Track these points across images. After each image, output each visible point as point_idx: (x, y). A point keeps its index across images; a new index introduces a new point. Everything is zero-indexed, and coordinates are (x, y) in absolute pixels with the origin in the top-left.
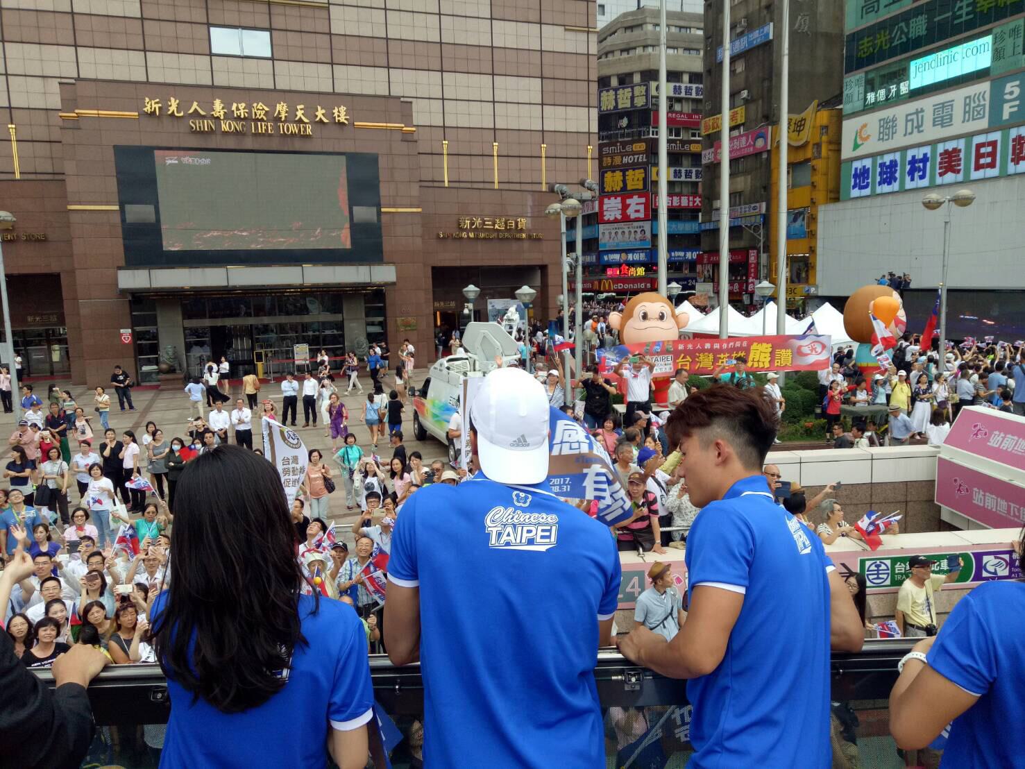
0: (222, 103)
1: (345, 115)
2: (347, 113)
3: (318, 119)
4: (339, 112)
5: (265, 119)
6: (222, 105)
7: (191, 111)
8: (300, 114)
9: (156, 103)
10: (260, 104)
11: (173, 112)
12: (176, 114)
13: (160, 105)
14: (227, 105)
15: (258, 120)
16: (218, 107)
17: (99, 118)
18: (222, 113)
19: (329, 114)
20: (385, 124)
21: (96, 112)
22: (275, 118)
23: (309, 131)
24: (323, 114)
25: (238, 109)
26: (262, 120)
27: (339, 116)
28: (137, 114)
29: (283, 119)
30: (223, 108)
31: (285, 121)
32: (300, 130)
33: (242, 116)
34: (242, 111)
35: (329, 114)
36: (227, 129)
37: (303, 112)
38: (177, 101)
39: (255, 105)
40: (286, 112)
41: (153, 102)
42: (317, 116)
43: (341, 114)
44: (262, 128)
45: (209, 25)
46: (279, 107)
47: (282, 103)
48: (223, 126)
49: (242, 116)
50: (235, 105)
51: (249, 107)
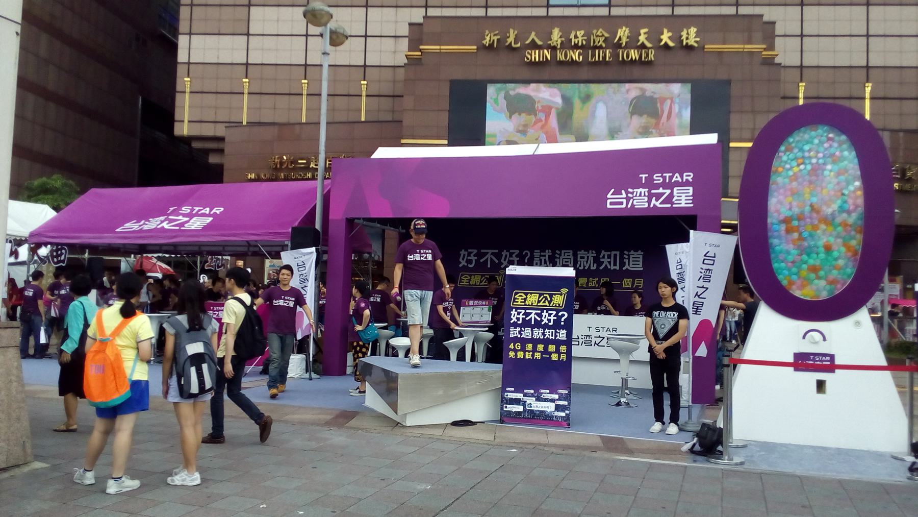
0: (560, 31)
1: (695, 37)
2: (698, 34)
3: (662, 43)
4: (688, 34)
5: (604, 45)
6: (560, 34)
7: (528, 42)
8: (642, 38)
9: (494, 35)
11: (511, 42)
13: (499, 37)
14: (565, 34)
15: (596, 47)
16: (556, 36)
17: (440, 54)
19: (678, 39)
20: (742, 46)
21: (438, 47)
23: (651, 57)
24: (669, 38)
26: (600, 47)
27: (687, 38)
28: (475, 47)
29: (624, 45)
30: (560, 37)
32: (641, 57)
33: (580, 44)
36: (563, 58)
38: (516, 32)
39: (595, 31)
40: (628, 37)
42: (661, 40)
43: (691, 36)
44: (598, 55)
47: (624, 28)
49: (580, 44)
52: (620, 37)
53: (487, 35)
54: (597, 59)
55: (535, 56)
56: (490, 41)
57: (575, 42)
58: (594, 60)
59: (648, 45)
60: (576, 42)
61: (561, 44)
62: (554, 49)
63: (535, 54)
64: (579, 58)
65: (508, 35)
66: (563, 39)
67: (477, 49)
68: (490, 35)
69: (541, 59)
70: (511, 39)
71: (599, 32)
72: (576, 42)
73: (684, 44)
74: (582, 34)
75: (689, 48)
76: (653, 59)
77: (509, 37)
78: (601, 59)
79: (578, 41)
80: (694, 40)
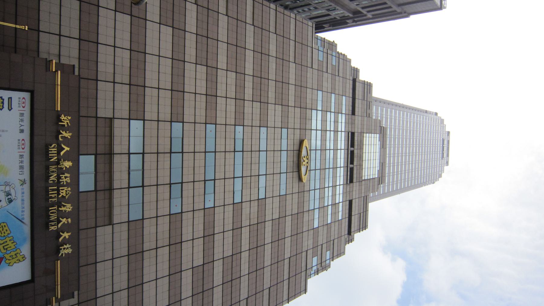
1: (65, 253)
3: (61, 234)
4: (67, 248)
5: (60, 196)
6: (68, 167)
8: (64, 220)
9: (67, 123)
10: (70, 193)
11: (62, 134)
12: (60, 136)
13: (66, 126)
14: (68, 170)
15: (58, 191)
16: (68, 164)
17: (54, 85)
18: (62, 166)
19: (64, 242)
20: (59, 283)
21: (59, 83)
22: (60, 203)
24: (65, 237)
25: (66, 177)
26: (58, 194)
27: (64, 249)
28: (59, 110)
29: (60, 209)
30: (66, 167)
31: (58, 210)
33: (61, 180)
34: (64, 180)
35: (64, 242)
36: (51, 170)
37: (66, 222)
38: (69, 137)
39: (69, 189)
40: (65, 211)
41: (68, 121)
43: (66, 250)
44: (53, 194)
45: (96, 155)
46: (69, 205)
48: (54, 167)
49: (61, 180)
50: (68, 175)
51: (68, 185)
52: (66, 206)
53: (67, 118)
54: (50, 193)
55: (53, 150)
56: (64, 120)
57: (62, 177)
58: (50, 190)
59: (60, 225)
60: (62, 178)
61: (61, 168)
62: (58, 163)
63: (54, 151)
64: (51, 181)
65: (67, 132)
66: (64, 169)
67: (58, 111)
68: (68, 119)
69: (50, 155)
70: (65, 134)
72: (62, 178)
73: (61, 248)
74: (67, 181)
75: (58, 251)
76: (50, 230)
77: (66, 132)
78: (50, 195)
79: (63, 179)
80: (63, 252)
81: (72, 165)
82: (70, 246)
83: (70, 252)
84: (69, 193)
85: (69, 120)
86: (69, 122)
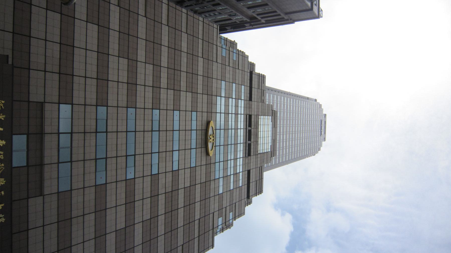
0: (3, 145)
10: (4, 168)
38: (3, 119)
41: (2, 105)
45: (28, 135)
47: (5, 181)
53: (1, 102)
68: (1, 103)
71: (3, 168)
81: (5, 143)
82: (3, 216)
83: (3, 221)
84: (2, 169)
85: (3, 104)
86: (3, 106)
